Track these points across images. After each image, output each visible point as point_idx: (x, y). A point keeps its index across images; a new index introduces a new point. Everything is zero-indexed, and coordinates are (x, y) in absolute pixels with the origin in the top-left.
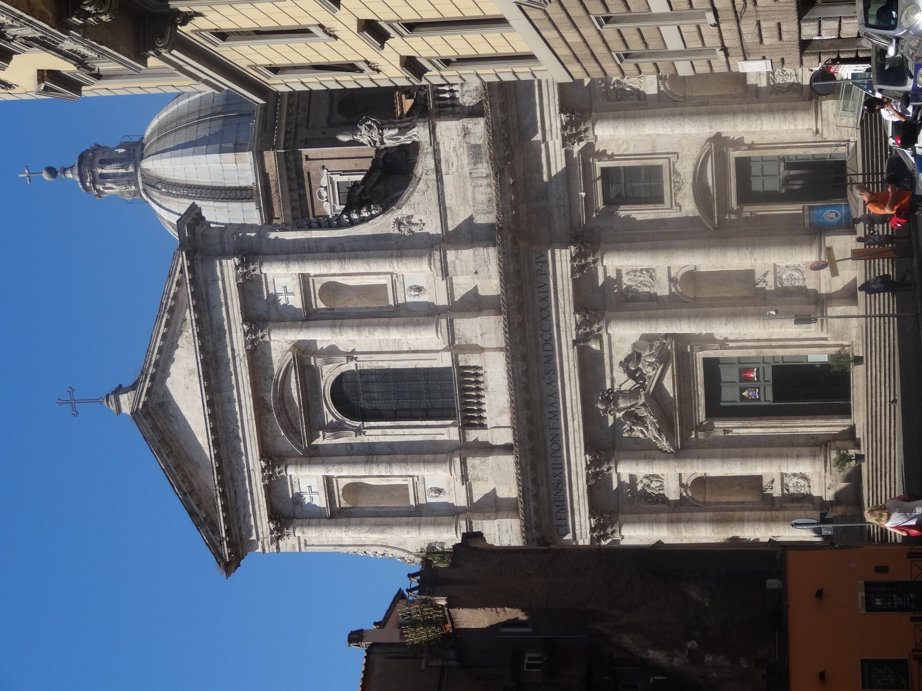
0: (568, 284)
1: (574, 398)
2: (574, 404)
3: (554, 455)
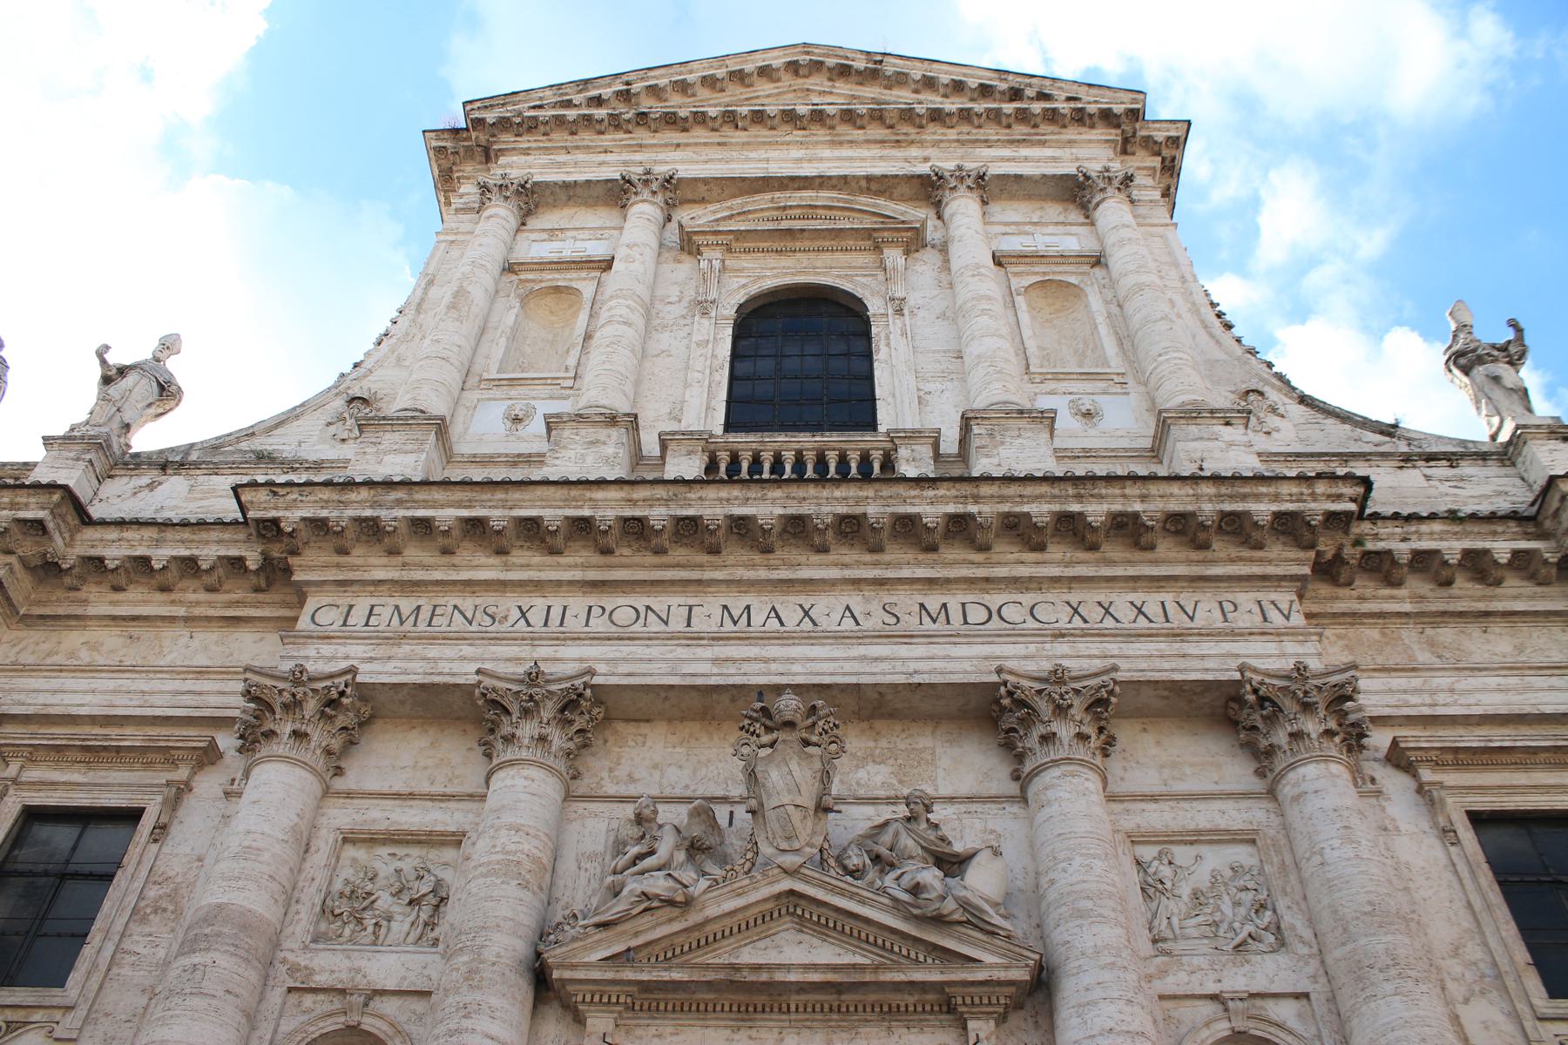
0: (1207, 670)
1: (797, 668)
2: (774, 667)
3: (596, 611)
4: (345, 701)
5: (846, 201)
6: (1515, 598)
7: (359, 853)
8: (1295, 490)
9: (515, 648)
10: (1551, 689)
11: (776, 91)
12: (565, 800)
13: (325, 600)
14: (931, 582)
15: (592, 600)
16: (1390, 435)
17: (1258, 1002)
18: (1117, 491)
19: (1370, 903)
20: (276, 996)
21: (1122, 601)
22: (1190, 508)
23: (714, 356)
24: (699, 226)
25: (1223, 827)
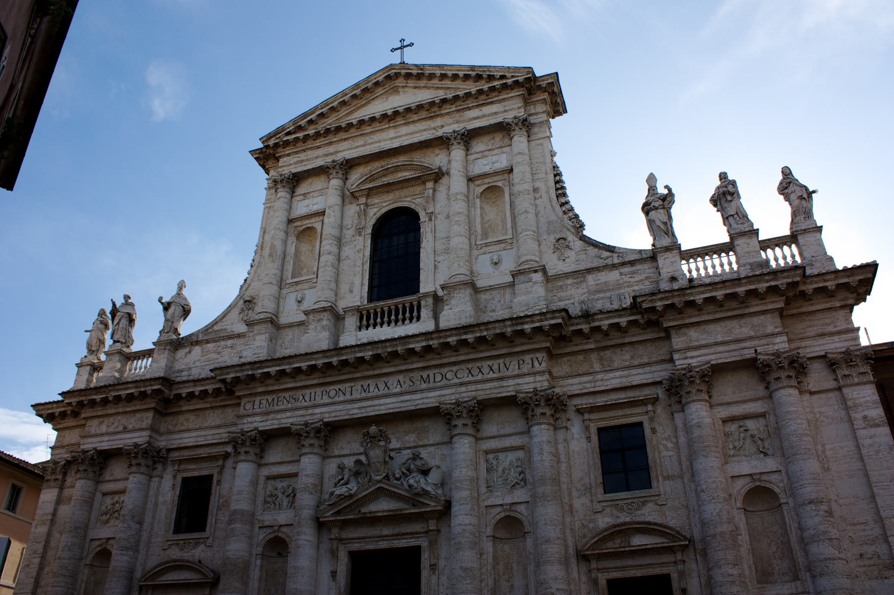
0: (509, 392)
1: (383, 408)
2: (376, 408)
4: (257, 438)
5: (409, 161)
6: (633, 336)
7: (273, 482)
8: (539, 318)
9: (302, 412)
10: (638, 374)
11: (384, 91)
12: (323, 459)
13: (247, 400)
14: (424, 368)
15: (322, 389)
16: (613, 252)
17: (515, 505)
18: (477, 329)
19: (542, 476)
20: (256, 529)
21: (485, 365)
22: (503, 331)
23: (364, 256)
24: (354, 188)
25: (514, 445)
